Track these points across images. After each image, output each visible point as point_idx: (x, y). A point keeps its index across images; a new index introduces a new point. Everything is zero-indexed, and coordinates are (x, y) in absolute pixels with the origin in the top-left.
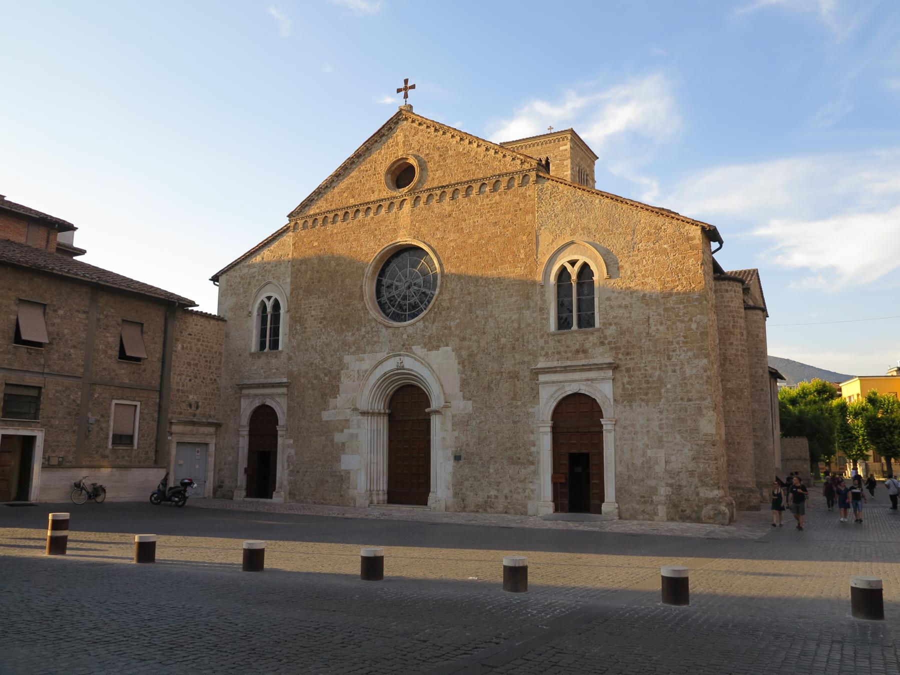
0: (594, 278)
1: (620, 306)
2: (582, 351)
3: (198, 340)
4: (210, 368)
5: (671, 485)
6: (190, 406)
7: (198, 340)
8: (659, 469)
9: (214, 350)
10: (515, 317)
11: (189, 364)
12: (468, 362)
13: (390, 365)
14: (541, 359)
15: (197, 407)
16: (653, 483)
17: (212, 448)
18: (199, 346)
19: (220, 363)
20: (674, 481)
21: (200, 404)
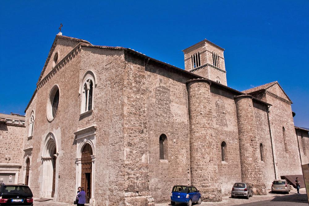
0: (93, 86)
1: (99, 98)
2: (88, 122)
3: (11, 134)
4: (17, 145)
5: (110, 189)
6: (6, 159)
7: (11, 134)
8: (107, 180)
9: (19, 138)
10: (74, 110)
11: (6, 143)
12: (63, 134)
13: (49, 138)
14: (79, 128)
15: (10, 160)
16: (104, 188)
17: (17, 175)
18: (12, 137)
19: (22, 142)
20: (111, 187)
21: (11, 158)
